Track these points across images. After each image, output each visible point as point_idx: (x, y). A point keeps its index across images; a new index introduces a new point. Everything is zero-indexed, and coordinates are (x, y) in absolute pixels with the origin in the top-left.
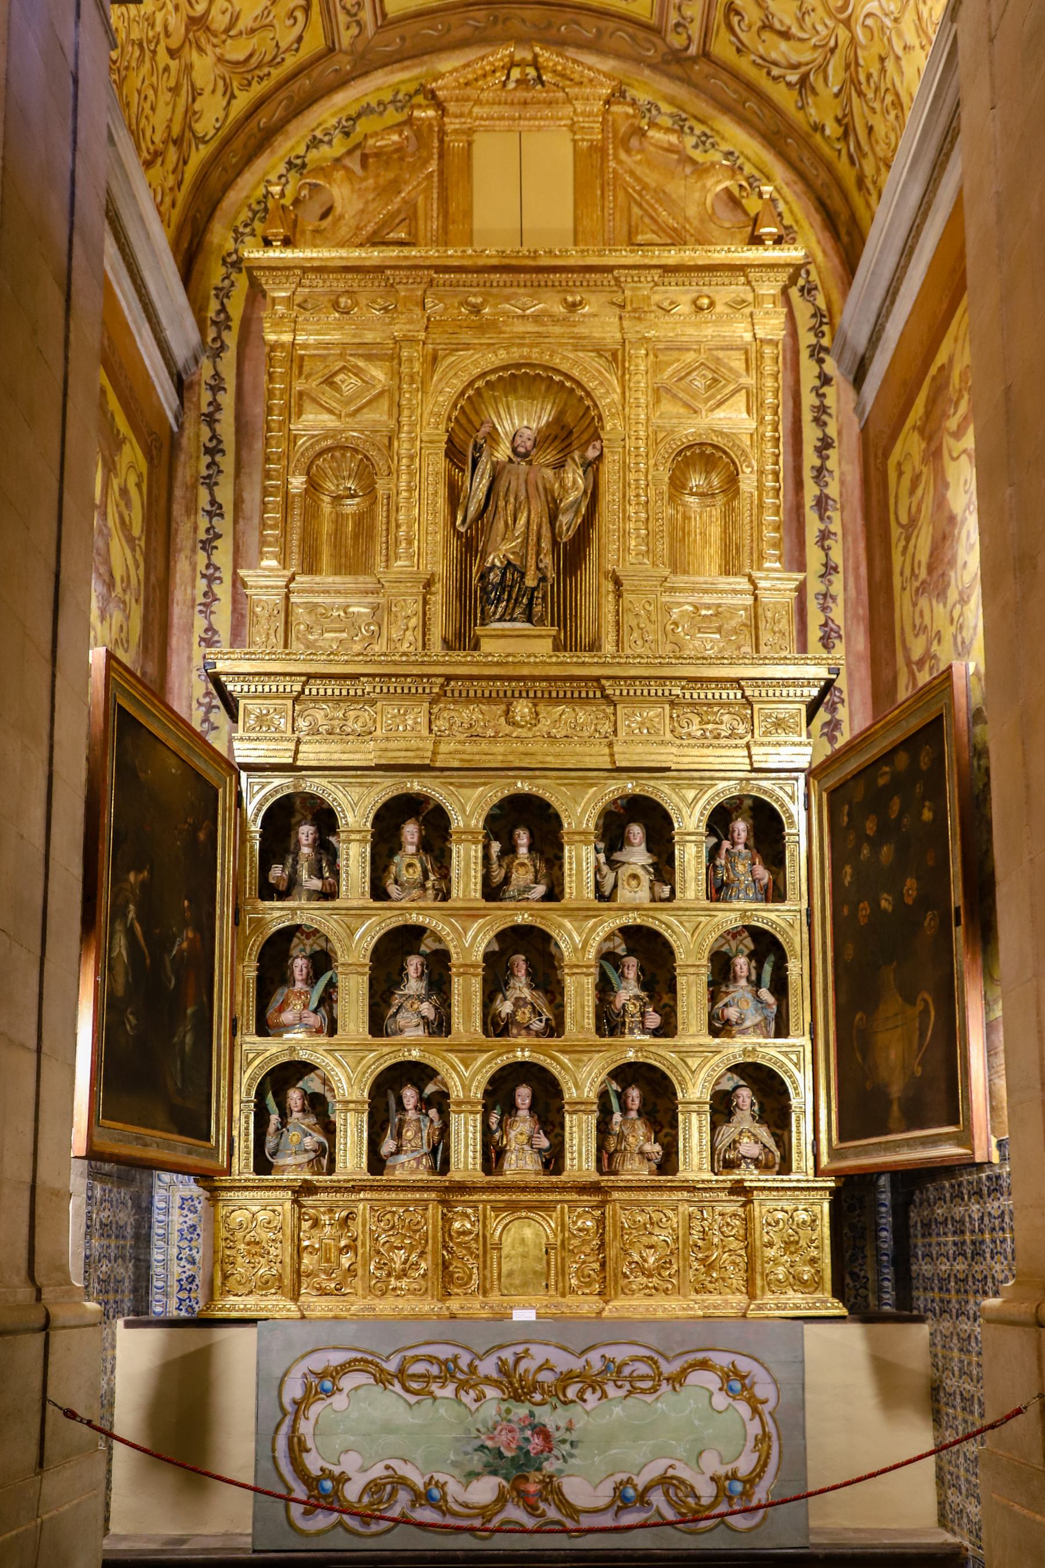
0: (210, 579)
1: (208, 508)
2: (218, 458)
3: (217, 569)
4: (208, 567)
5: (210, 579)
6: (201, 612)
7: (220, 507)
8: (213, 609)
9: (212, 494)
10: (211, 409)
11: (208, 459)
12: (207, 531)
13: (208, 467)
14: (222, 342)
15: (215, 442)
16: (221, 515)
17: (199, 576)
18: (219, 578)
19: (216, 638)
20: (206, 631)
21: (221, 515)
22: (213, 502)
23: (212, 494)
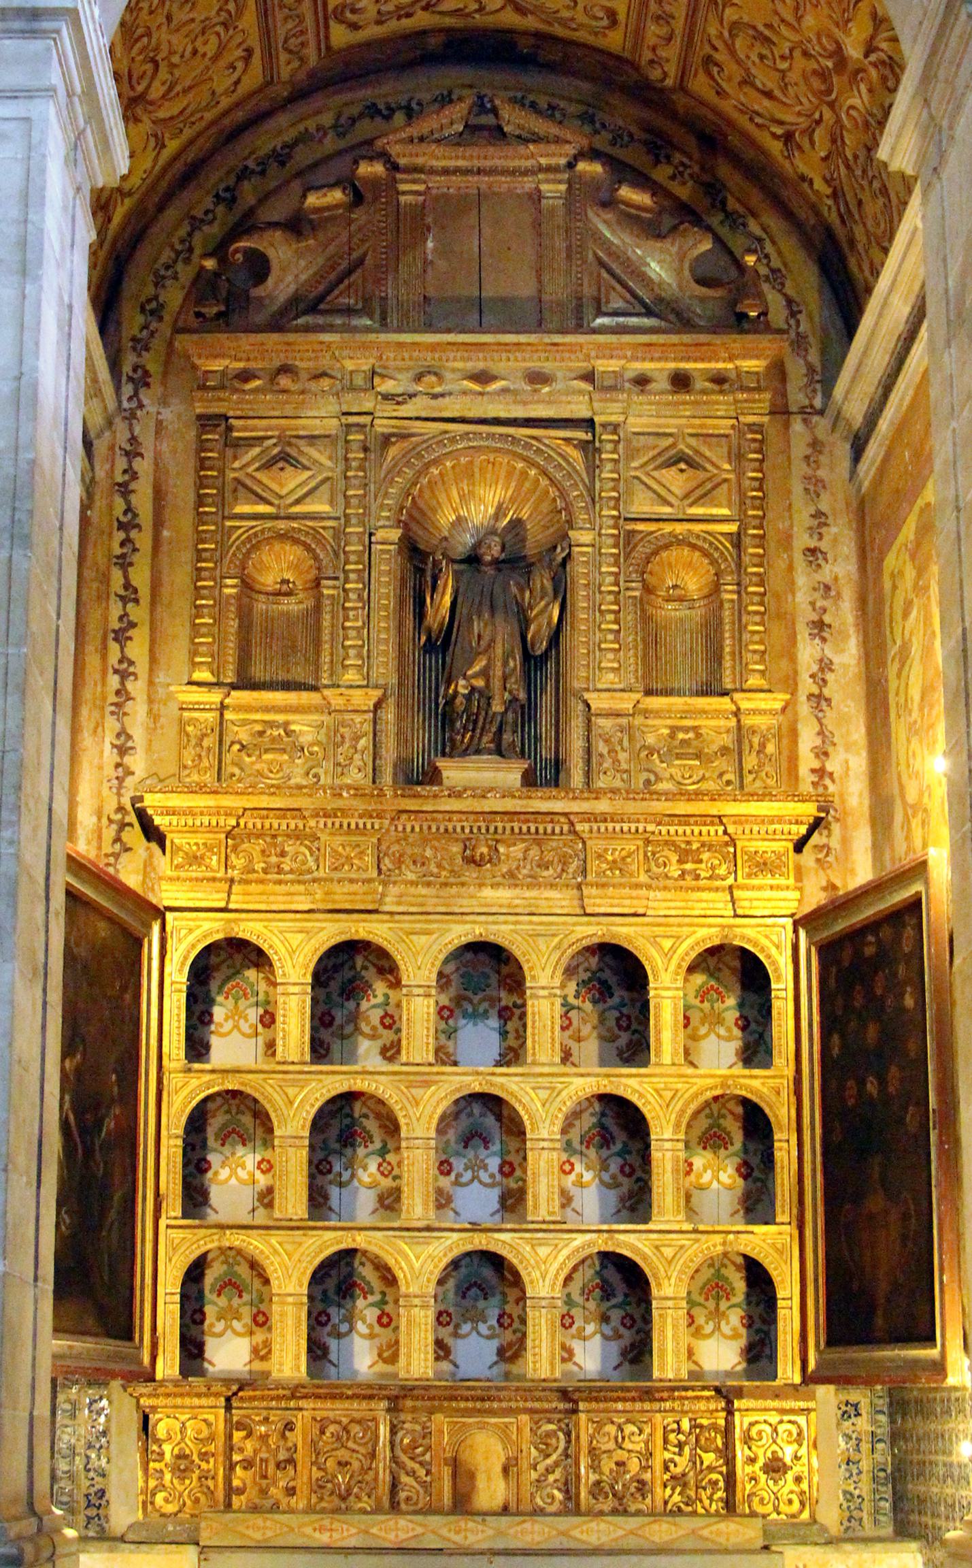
0: (124, 675)
1: (122, 592)
2: (134, 534)
3: (131, 663)
4: (120, 662)
5: (124, 675)
6: (112, 713)
7: (136, 591)
8: (126, 710)
9: (126, 577)
10: (127, 477)
11: (121, 535)
12: (121, 618)
13: (122, 544)
14: (139, 401)
15: (130, 515)
16: (136, 601)
17: (111, 671)
18: (134, 674)
19: (130, 744)
20: (118, 736)
21: (136, 601)
22: (127, 585)
23: (126, 577)
